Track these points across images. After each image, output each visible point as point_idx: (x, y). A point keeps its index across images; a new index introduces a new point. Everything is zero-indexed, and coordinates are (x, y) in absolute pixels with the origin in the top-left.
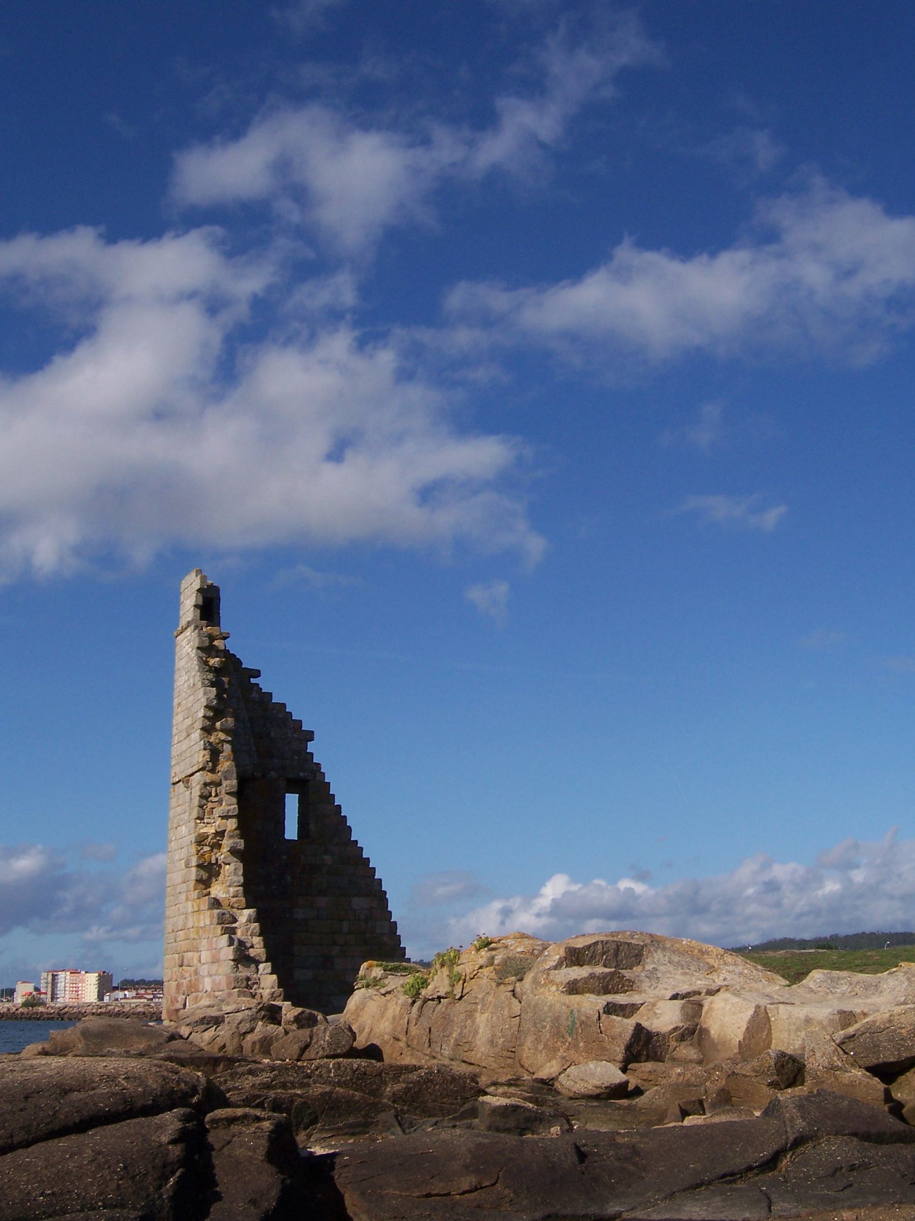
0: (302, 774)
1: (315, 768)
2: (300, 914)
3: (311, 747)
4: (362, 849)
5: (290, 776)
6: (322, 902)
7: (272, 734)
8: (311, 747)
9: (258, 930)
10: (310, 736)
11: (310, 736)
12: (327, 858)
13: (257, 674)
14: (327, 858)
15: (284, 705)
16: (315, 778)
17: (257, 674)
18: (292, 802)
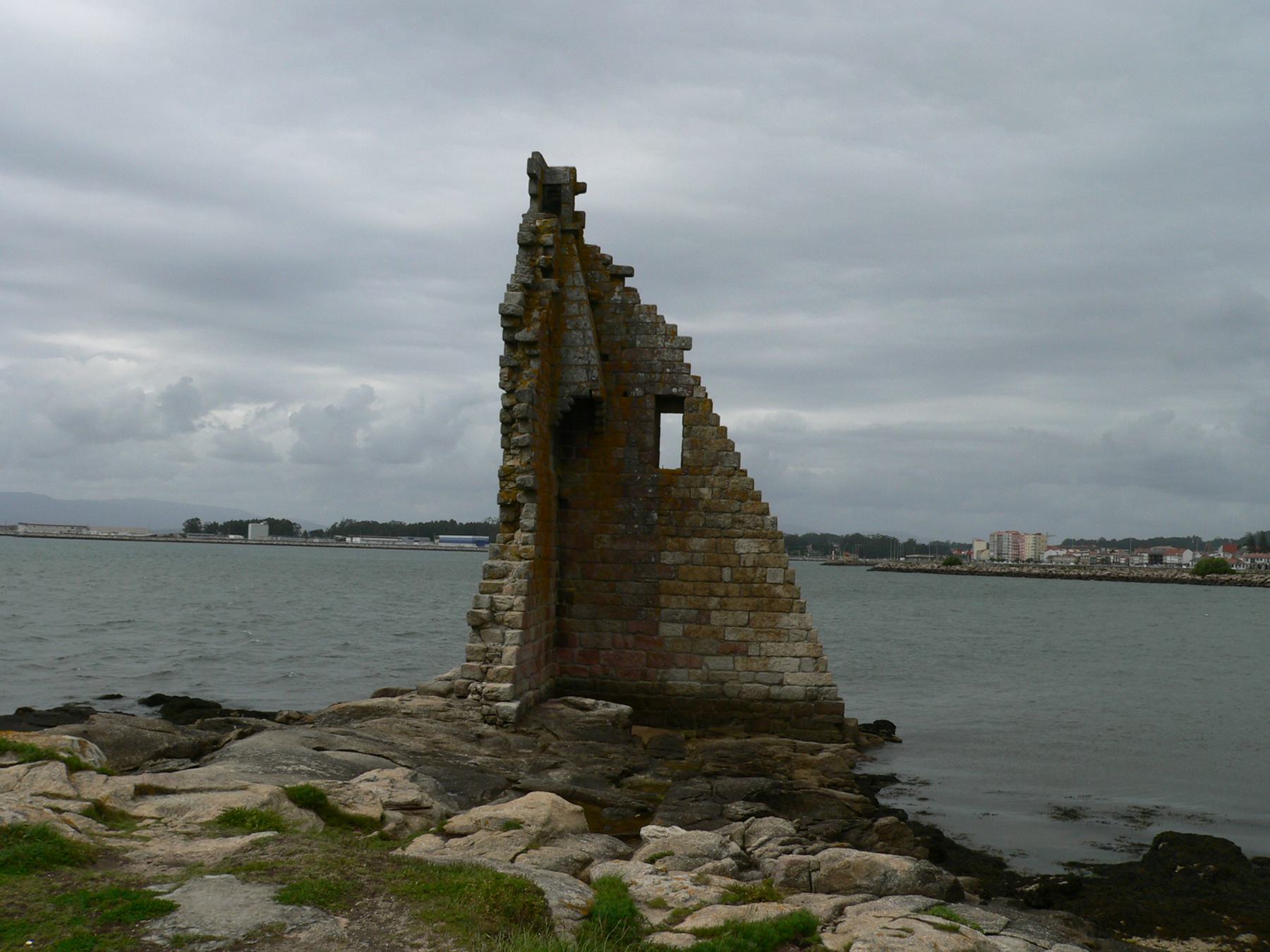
0: (674, 390)
1: (692, 382)
2: (668, 558)
3: (688, 357)
4: (752, 481)
5: (660, 393)
6: (697, 543)
7: (638, 343)
8: (688, 357)
9: (524, 588)
10: (687, 344)
11: (687, 344)
12: (705, 491)
13: (630, 272)
14: (705, 491)
15: (655, 307)
16: (692, 395)
17: (630, 272)
18: (671, 424)
